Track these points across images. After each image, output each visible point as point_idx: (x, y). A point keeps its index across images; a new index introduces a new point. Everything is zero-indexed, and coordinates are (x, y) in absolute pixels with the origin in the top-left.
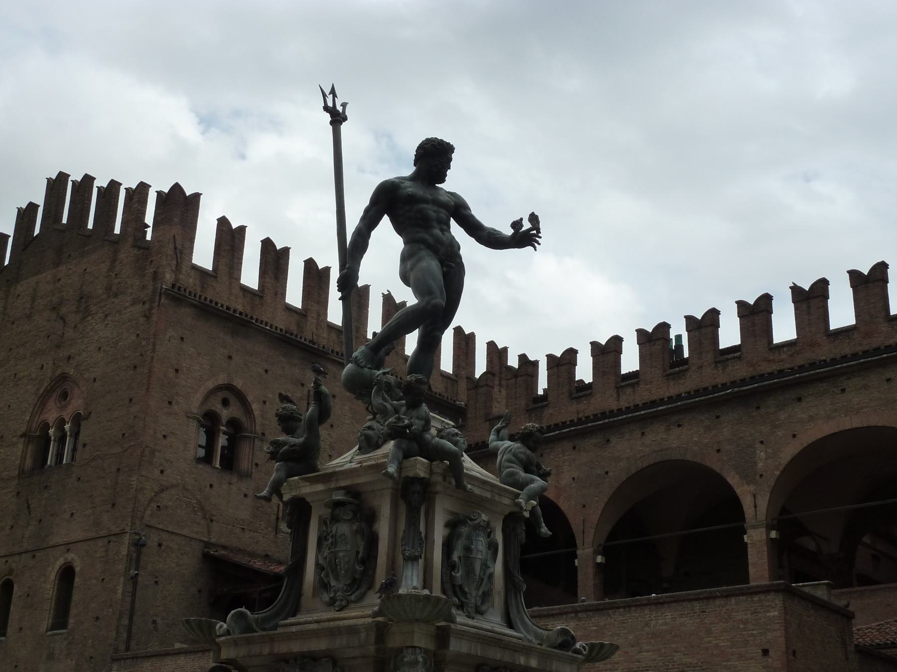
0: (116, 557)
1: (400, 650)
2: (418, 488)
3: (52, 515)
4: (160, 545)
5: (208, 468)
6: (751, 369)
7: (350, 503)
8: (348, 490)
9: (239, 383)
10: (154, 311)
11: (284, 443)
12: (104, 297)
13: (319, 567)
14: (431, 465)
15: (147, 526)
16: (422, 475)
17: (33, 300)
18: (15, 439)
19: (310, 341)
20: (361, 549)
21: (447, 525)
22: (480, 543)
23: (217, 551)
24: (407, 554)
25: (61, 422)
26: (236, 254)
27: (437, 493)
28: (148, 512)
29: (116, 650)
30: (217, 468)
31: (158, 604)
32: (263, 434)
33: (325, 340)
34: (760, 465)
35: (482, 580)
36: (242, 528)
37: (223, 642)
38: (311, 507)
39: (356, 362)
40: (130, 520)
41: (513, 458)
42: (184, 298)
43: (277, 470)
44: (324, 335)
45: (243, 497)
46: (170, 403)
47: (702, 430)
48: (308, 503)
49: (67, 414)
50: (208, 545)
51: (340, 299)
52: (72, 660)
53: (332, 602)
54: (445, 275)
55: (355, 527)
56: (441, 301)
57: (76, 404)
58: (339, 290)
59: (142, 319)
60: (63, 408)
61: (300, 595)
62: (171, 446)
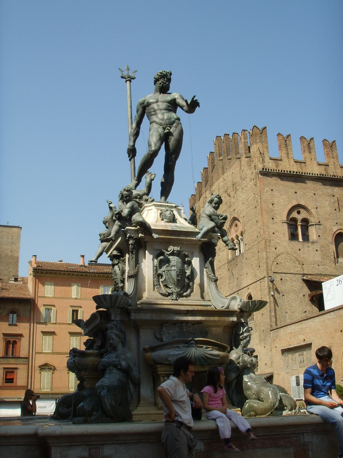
0: (264, 288)
3: (240, 276)
4: (281, 279)
5: (296, 242)
9: (302, 203)
10: (258, 182)
12: (240, 182)
15: (274, 273)
17: (219, 190)
18: (224, 248)
19: (333, 176)
23: (308, 277)
25: (237, 237)
26: (288, 148)
28: (273, 267)
29: (271, 326)
30: (301, 241)
31: (286, 304)
32: (319, 222)
36: (319, 265)
40: (266, 271)
42: (269, 173)
44: (339, 171)
45: (316, 251)
46: (273, 219)
49: (239, 233)
50: (304, 275)
52: (257, 333)
57: (240, 228)
59: (254, 187)
60: (236, 231)
62: (278, 237)
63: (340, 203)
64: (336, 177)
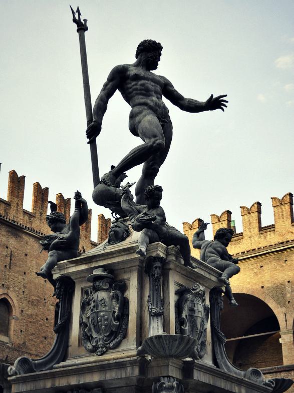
1: (158, 380)
2: (158, 264)
6: (282, 238)
7: (106, 277)
8: (104, 267)
11: (56, 238)
13: (83, 324)
14: (168, 249)
16: (162, 255)
19: (12, 221)
20: (117, 310)
21: (177, 293)
22: (200, 306)
24: (154, 312)
27: (170, 269)
33: (22, 220)
34: (288, 295)
35: (202, 332)
37: (14, 380)
38: (74, 283)
39: (104, 183)
41: (214, 251)
43: (51, 256)
44: (21, 217)
47: (252, 276)
48: (72, 280)
51: (88, 143)
53: (94, 350)
54: (163, 126)
55: (112, 294)
56: (160, 141)
58: (88, 137)
61: (67, 346)
63: (13, 259)
64: (16, 224)
